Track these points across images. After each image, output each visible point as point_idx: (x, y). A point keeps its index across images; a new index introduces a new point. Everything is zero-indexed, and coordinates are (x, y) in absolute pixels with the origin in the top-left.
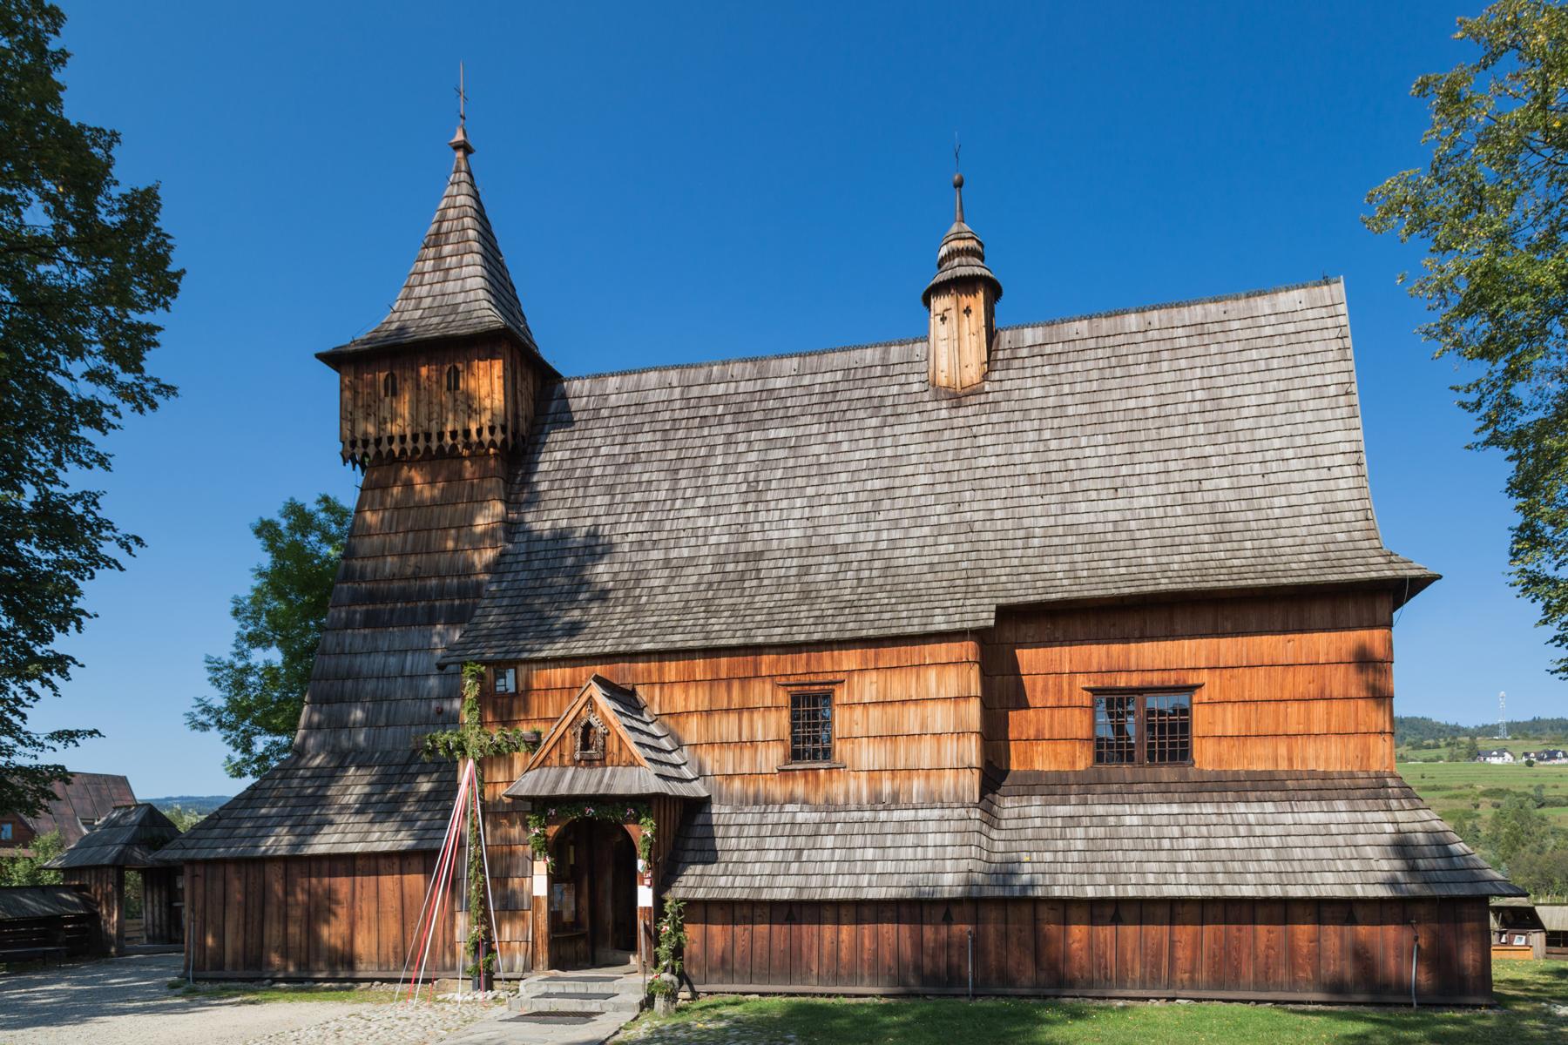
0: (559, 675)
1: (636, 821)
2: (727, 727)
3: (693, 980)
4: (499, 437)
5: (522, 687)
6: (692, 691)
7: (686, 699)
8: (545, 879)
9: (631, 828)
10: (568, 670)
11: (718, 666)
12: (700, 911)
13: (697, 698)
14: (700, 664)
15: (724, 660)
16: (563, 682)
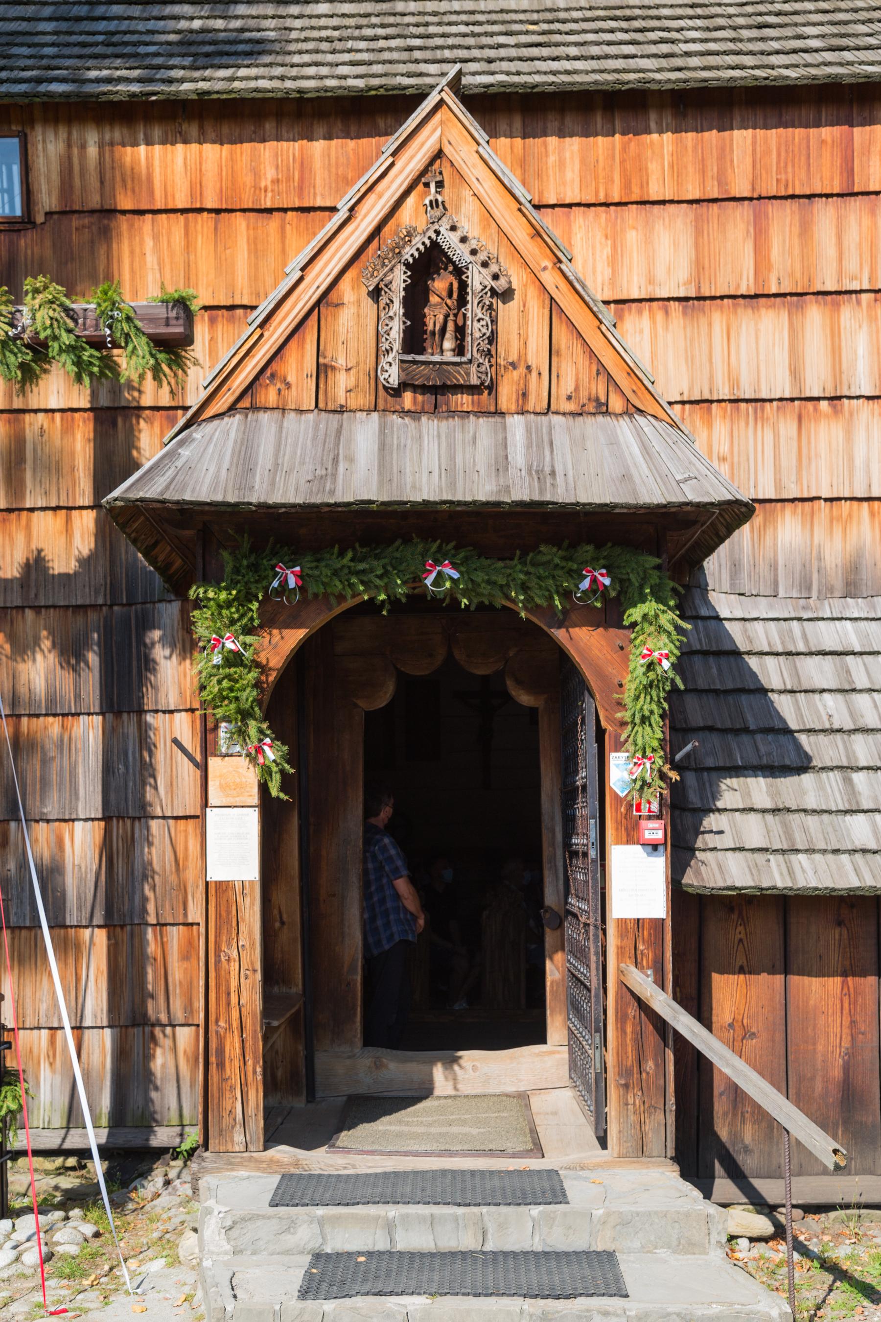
0: (171, 166)
1: (610, 614)
2: (760, 351)
3: (747, 1163)
5: (48, 199)
6: (632, 237)
7: (614, 261)
8: (250, 822)
9: (585, 643)
10: (212, 154)
11: (724, 154)
12: (764, 932)
13: (662, 253)
14: (665, 155)
15: (742, 139)
16: (197, 187)
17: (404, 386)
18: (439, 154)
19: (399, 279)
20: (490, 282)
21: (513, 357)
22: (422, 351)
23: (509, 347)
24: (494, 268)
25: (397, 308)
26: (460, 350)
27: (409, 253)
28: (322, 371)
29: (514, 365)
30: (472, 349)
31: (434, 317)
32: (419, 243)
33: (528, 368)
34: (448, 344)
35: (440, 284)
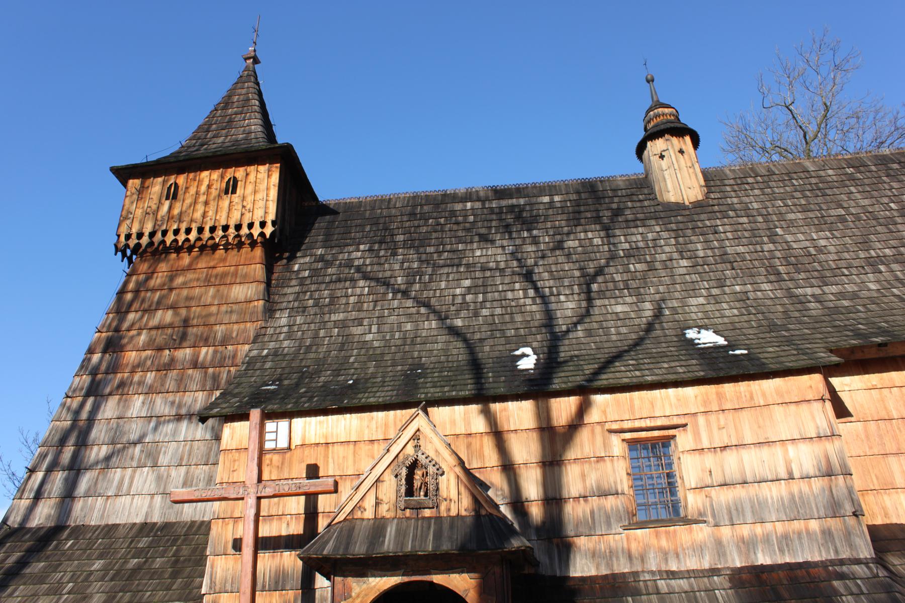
4: (269, 230)
17: (405, 508)
18: (418, 430)
19: (404, 472)
20: (436, 471)
21: (445, 496)
22: (412, 495)
23: (443, 492)
24: (437, 466)
25: (403, 481)
26: (426, 495)
27: (408, 463)
28: (377, 504)
29: (446, 500)
30: (430, 494)
31: (417, 484)
32: (411, 460)
33: (451, 500)
34: (422, 493)
35: (418, 474)
